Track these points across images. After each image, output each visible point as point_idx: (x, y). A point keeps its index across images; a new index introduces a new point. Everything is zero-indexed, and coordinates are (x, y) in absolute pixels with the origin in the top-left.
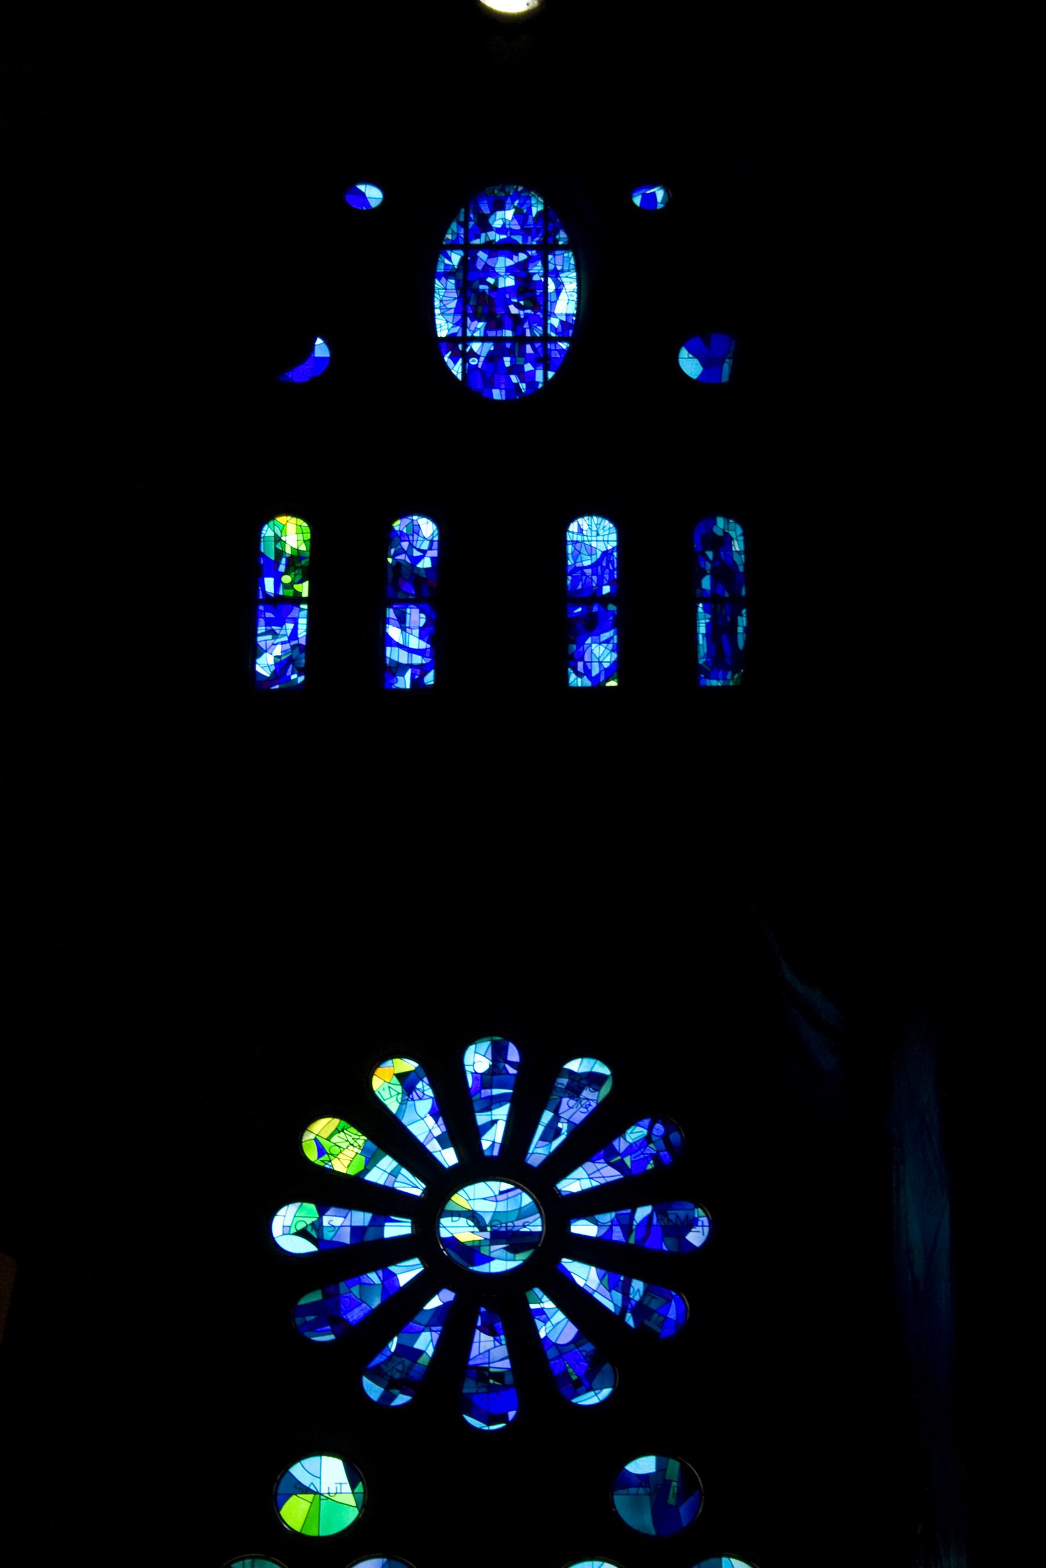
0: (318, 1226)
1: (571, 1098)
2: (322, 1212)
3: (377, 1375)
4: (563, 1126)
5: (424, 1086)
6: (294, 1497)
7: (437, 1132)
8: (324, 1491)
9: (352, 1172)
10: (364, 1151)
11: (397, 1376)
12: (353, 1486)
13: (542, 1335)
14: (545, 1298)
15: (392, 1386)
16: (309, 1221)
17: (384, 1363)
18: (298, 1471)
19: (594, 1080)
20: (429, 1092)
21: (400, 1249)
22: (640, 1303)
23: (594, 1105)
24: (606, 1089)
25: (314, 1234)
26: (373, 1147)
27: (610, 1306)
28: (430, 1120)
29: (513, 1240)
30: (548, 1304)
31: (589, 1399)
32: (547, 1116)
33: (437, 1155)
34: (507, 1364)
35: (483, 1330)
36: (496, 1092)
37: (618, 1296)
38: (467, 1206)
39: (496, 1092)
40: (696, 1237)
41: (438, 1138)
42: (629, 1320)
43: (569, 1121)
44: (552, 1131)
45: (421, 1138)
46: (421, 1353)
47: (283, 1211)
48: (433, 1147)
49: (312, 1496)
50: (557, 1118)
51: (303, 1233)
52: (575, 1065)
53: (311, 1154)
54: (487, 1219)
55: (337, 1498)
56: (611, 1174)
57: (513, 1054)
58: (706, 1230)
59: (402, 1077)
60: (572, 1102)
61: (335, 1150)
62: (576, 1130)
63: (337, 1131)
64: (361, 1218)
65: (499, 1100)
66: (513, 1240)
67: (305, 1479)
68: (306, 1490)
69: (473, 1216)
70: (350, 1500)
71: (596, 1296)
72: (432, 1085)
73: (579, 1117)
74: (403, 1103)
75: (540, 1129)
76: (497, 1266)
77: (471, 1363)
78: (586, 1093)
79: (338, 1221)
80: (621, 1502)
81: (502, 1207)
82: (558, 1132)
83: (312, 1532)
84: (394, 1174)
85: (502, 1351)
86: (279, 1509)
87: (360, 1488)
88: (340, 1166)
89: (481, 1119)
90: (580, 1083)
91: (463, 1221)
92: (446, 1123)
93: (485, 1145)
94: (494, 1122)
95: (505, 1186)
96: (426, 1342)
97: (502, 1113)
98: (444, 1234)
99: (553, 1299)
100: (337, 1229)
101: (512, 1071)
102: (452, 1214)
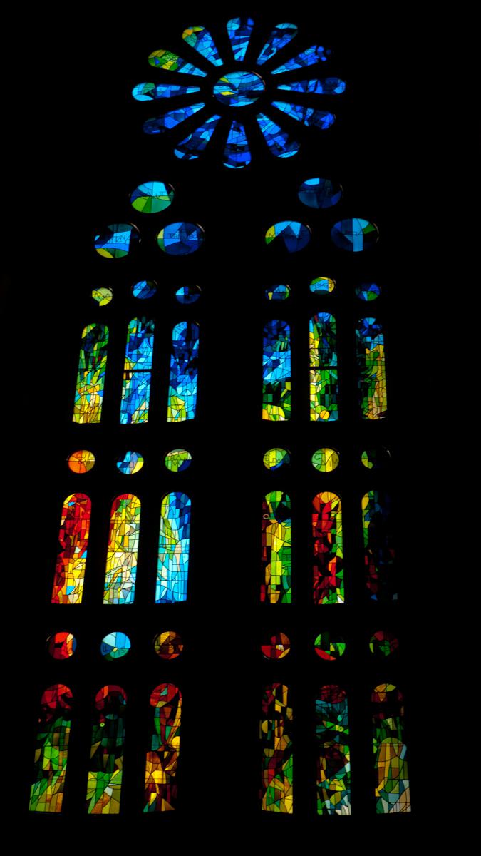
0: (155, 91)
1: (278, 38)
2: (156, 86)
3: (181, 149)
4: (274, 49)
5: (208, 36)
6: (139, 198)
7: (214, 53)
8: (154, 195)
9: (173, 69)
10: (178, 61)
11: (191, 149)
12: (169, 192)
13: (263, 131)
14: (264, 117)
15: (188, 153)
16: (151, 89)
17: (186, 143)
18: (144, 188)
19: (288, 31)
20: (210, 38)
21: (194, 99)
22: (311, 117)
23: (289, 40)
24: (294, 35)
25: (153, 94)
26: (182, 60)
27: (297, 118)
28: (210, 49)
29: (250, 94)
30: (266, 119)
31: (286, 155)
32: (267, 46)
33: (214, 63)
34: (246, 143)
35: (234, 129)
36: (242, 37)
37: (301, 115)
38: (227, 81)
39: (242, 37)
40: (338, 91)
41: (215, 56)
42: (306, 123)
43: (277, 47)
44: (269, 51)
45: (206, 56)
46: (204, 140)
47: (138, 86)
48: (211, 59)
49: (147, 198)
50: (271, 46)
51: (147, 94)
52: (280, 26)
53: (153, 64)
54: (237, 86)
55: (161, 198)
56: (298, 66)
57: (250, 22)
58: (344, 88)
59: (197, 33)
60: (279, 40)
61: (163, 62)
62: (279, 51)
63: (165, 54)
64: (175, 88)
65: (244, 40)
66: (250, 94)
67: (145, 192)
68: (146, 195)
69: (231, 86)
70: (167, 199)
71: (290, 115)
72: (211, 35)
73: (282, 45)
74: (197, 43)
75: (263, 51)
76: (241, 104)
77: (228, 143)
78: (285, 36)
79: (164, 89)
80: (302, 197)
81: (244, 81)
82: (272, 52)
83: (148, 211)
84: (192, 70)
85: (244, 138)
86: (131, 203)
87: (172, 193)
88: (166, 67)
89: (235, 48)
90: (281, 33)
91: (225, 87)
92: (218, 49)
93: (236, 57)
94: (241, 49)
95: (245, 74)
96: (206, 136)
97: (245, 45)
98: (215, 92)
99: (268, 116)
100: (164, 92)
101: (250, 29)
102: (220, 85)
